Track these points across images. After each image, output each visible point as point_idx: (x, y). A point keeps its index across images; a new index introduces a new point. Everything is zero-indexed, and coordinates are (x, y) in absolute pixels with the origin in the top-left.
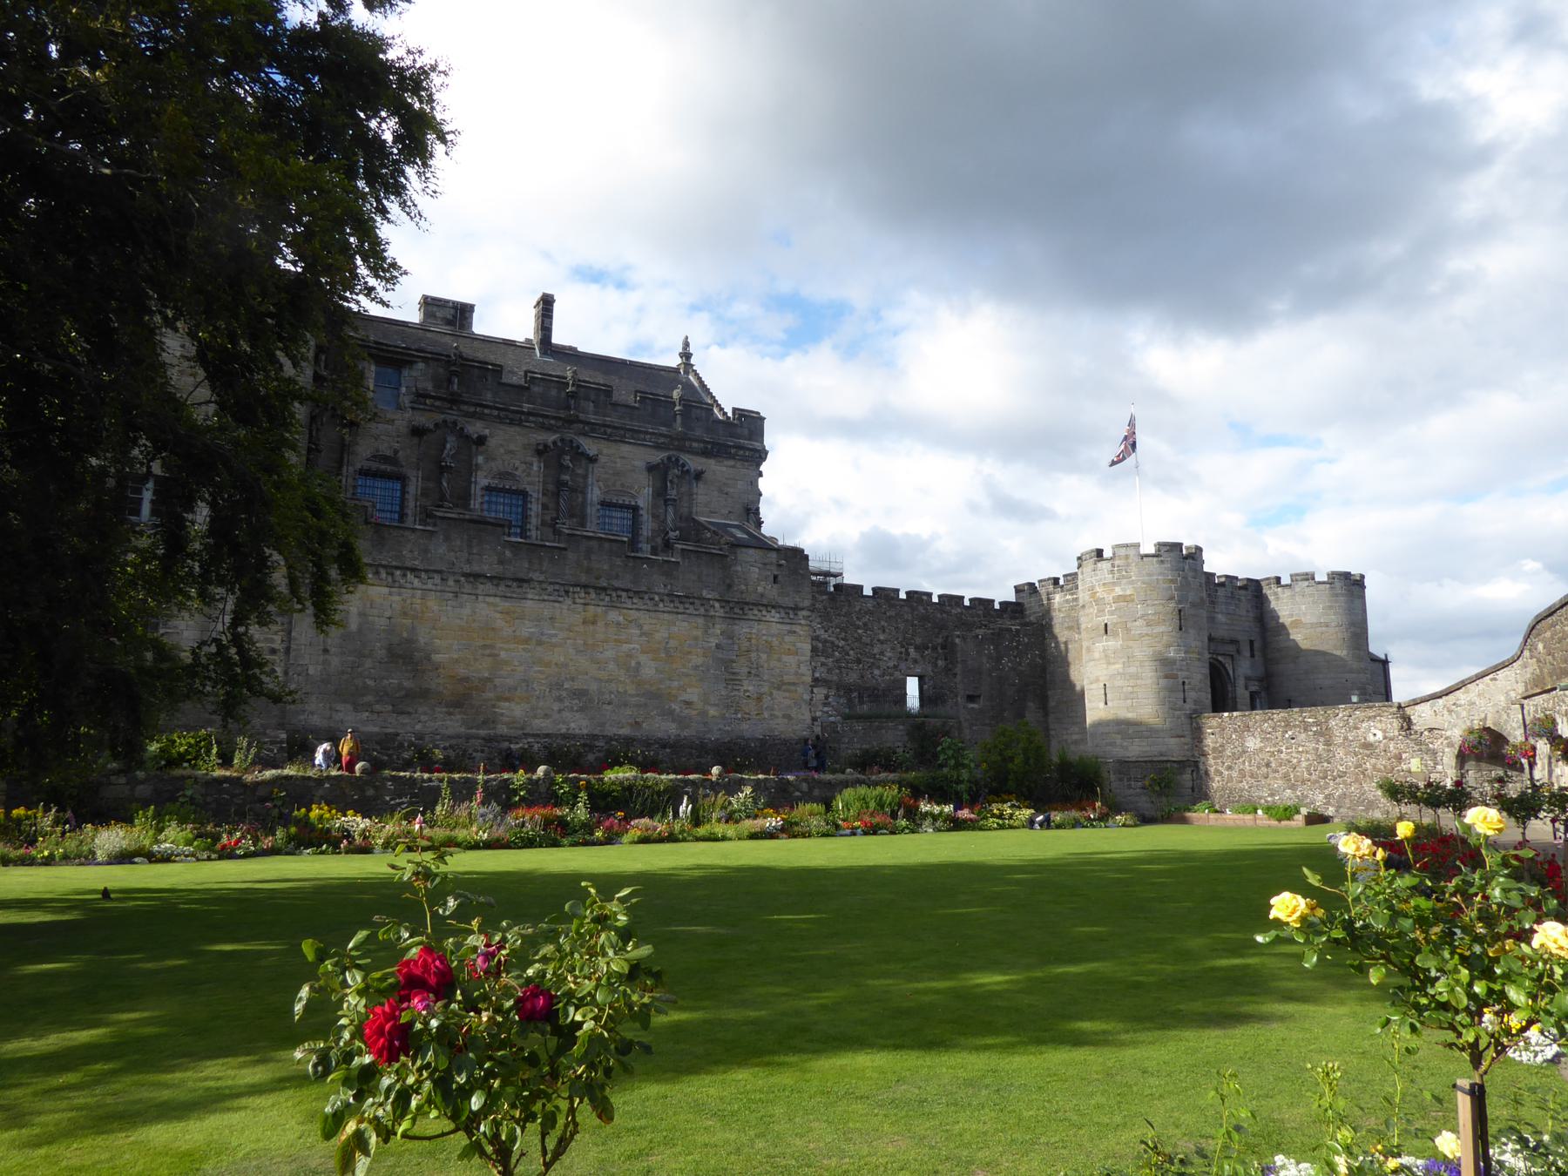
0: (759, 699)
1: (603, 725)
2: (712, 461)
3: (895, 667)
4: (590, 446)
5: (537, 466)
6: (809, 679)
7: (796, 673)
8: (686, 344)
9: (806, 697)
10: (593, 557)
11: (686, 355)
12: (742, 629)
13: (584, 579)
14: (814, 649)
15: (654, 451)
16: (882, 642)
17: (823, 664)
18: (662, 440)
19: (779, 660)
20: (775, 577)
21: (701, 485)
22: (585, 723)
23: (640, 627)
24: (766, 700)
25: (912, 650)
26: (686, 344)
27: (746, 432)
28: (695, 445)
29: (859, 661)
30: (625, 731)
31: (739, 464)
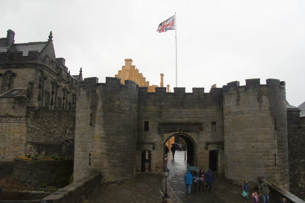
0: (5, 149)
2: (20, 70)
3: (60, 137)
6: (25, 142)
7: (20, 140)
8: (51, 33)
9: (24, 148)
11: (51, 37)
14: (28, 131)
15: (3, 70)
16: (55, 128)
17: (31, 136)
18: (4, 66)
19: (13, 135)
20: (13, 107)
21: (16, 78)
24: (7, 149)
25: (68, 130)
26: (51, 33)
28: (13, 65)
29: (45, 135)
31: (29, 69)
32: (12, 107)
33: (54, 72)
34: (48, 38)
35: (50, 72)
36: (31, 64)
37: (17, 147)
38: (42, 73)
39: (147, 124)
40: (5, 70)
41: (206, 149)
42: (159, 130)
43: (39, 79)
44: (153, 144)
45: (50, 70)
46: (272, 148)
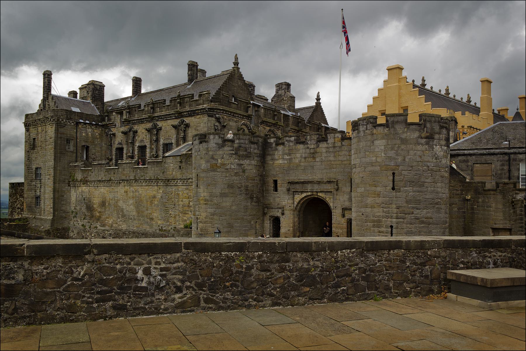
0: (175, 217)
1: (129, 226)
2: (193, 118)
4: (160, 124)
5: (148, 136)
8: (236, 58)
10: (126, 170)
11: (236, 64)
12: (169, 189)
13: (124, 178)
15: (175, 120)
19: (182, 201)
20: (180, 166)
22: (125, 225)
23: (139, 192)
26: (236, 58)
27: (201, 101)
30: (135, 229)
32: (178, 167)
33: (241, 115)
34: (233, 66)
35: (233, 116)
36: (202, 109)
37: (187, 215)
38: (218, 120)
39: (275, 182)
40: (179, 120)
41: (344, 216)
42: (288, 190)
43: (213, 127)
44: (283, 208)
45: (231, 112)
46: (387, 217)
